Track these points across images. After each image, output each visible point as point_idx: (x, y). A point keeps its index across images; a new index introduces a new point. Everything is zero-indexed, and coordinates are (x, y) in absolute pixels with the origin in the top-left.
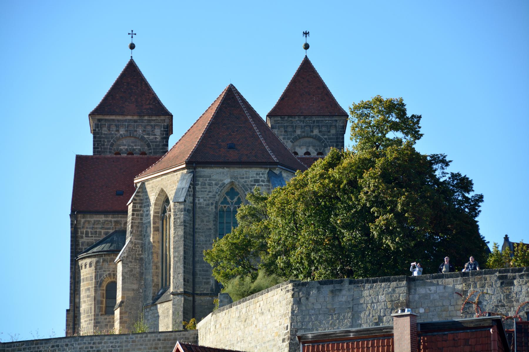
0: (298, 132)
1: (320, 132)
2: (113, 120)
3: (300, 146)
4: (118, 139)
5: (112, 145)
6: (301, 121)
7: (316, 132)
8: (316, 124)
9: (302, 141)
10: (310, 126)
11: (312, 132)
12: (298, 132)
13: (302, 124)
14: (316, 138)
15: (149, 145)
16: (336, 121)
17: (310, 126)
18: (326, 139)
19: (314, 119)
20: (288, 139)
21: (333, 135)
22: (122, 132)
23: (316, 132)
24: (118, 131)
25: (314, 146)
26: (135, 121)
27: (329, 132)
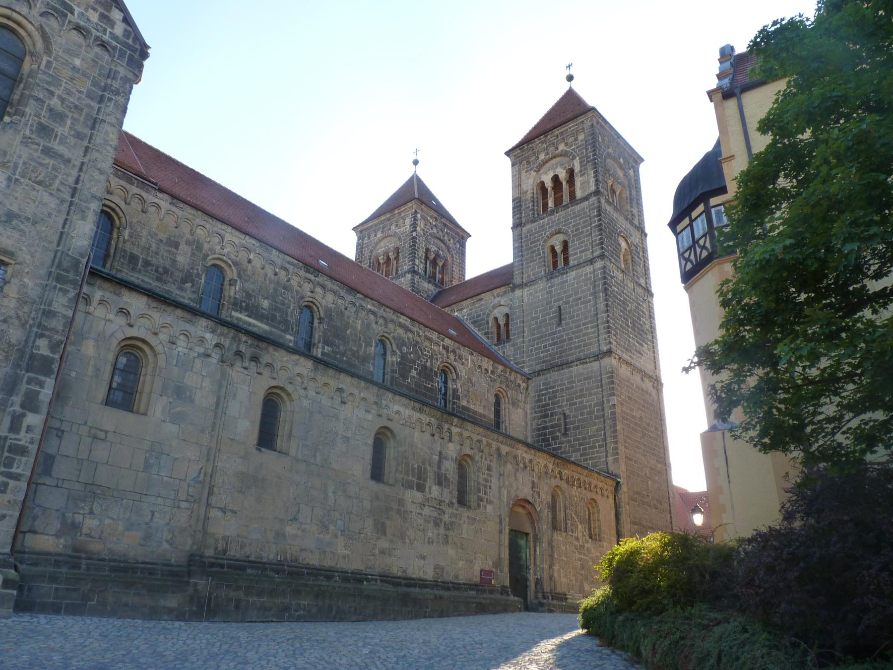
0: (542, 157)
1: (566, 144)
2: (371, 227)
3: (546, 173)
4: (377, 244)
5: (371, 252)
6: (542, 143)
7: (562, 147)
8: (560, 138)
9: (548, 165)
10: (553, 144)
11: (557, 148)
12: (542, 157)
13: (545, 145)
14: (564, 154)
15: (400, 239)
16: (583, 122)
17: (553, 144)
18: (573, 150)
19: (556, 132)
20: (531, 170)
21: (582, 141)
22: (379, 235)
23: (562, 147)
24: (376, 235)
25: (561, 165)
26: (389, 219)
27: (576, 139)
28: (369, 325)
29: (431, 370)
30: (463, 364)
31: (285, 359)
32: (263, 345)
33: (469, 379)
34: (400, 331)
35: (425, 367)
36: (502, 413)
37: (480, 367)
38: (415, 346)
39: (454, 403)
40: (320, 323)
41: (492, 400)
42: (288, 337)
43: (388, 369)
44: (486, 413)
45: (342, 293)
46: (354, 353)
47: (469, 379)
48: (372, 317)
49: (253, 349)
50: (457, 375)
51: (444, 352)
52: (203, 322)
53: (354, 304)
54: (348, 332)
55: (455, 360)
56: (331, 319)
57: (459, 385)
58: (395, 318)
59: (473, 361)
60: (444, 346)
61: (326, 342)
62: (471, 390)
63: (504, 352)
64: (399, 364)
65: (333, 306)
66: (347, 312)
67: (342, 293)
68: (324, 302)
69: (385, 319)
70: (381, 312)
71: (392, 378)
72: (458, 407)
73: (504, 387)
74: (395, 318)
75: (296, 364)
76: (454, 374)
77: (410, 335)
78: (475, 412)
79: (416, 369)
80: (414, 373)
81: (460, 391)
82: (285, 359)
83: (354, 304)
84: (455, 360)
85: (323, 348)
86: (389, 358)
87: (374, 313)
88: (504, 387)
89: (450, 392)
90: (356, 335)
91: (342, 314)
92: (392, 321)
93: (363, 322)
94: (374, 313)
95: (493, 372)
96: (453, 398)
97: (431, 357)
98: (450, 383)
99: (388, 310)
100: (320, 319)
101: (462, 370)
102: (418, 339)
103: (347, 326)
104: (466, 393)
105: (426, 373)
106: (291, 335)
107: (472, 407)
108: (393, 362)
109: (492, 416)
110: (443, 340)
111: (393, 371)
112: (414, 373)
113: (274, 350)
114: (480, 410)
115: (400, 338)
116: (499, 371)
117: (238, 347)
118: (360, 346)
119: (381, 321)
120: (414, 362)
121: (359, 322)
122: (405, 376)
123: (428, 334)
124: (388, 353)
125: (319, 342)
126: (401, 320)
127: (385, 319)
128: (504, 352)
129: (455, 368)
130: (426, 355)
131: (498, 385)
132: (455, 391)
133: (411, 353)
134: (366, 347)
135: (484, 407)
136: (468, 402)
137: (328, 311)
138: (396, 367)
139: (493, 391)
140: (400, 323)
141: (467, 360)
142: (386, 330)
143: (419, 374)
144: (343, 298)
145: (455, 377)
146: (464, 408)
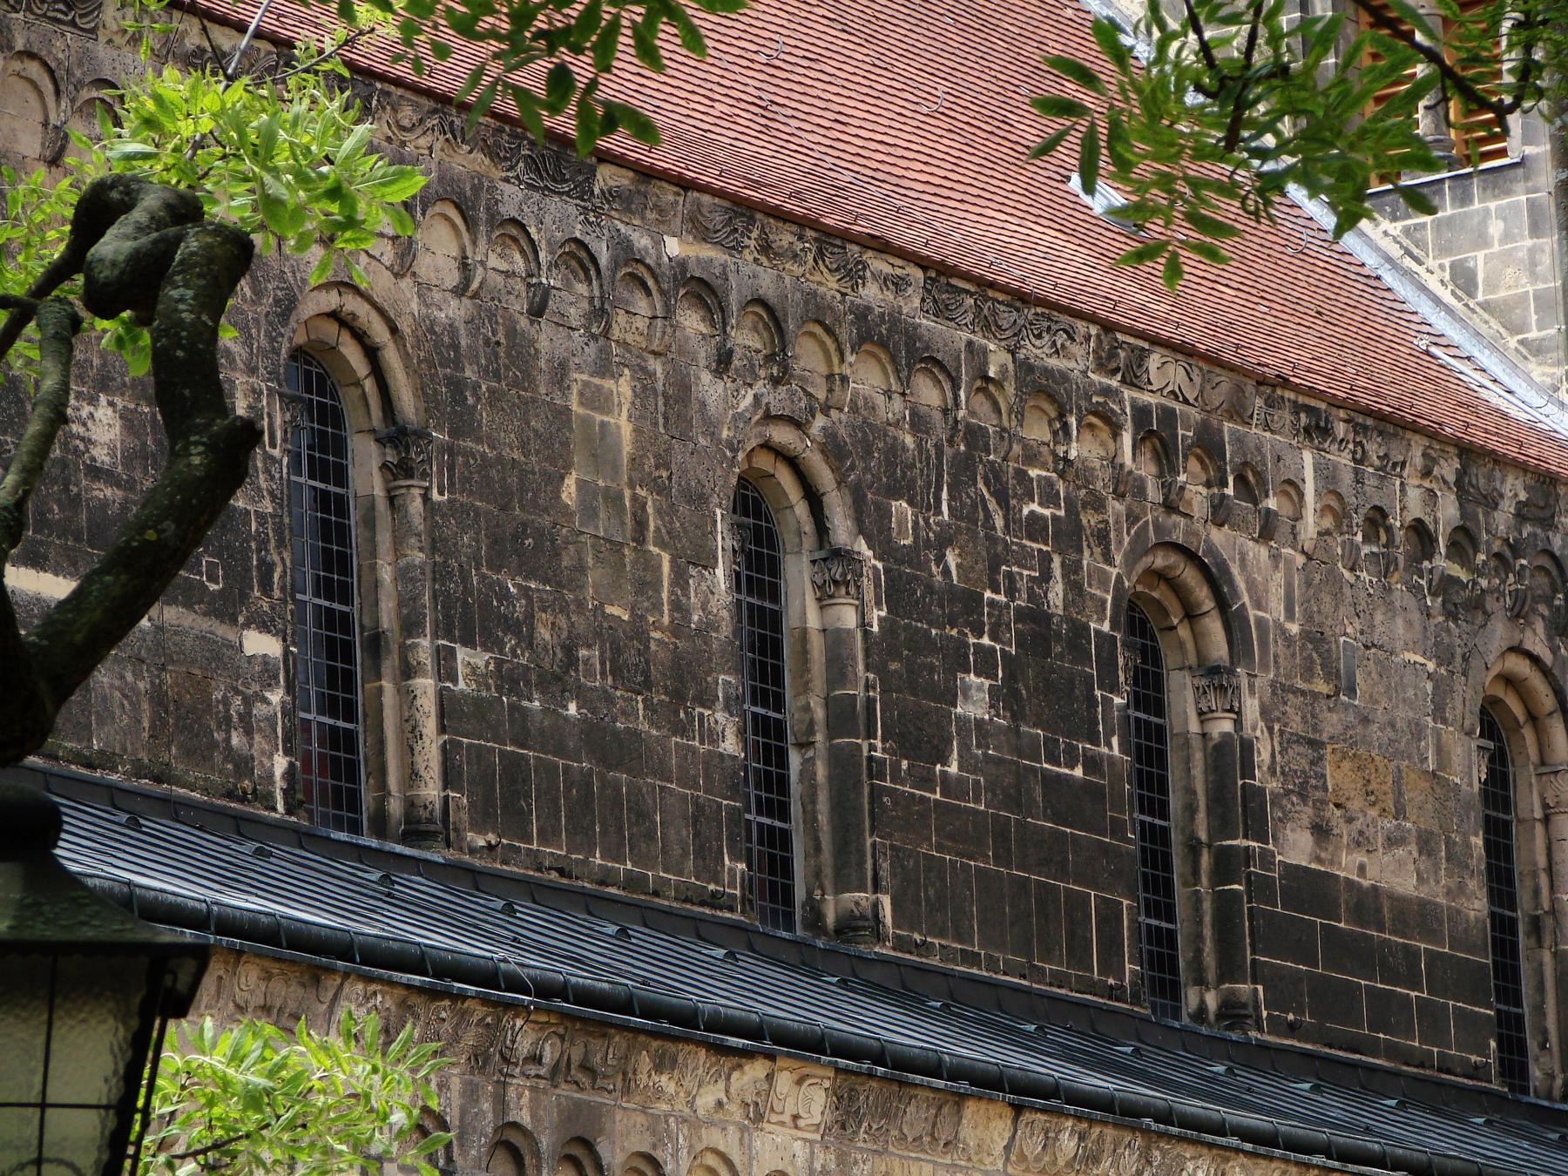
28: (682, 391)
29: (1080, 630)
30: (1266, 533)
31: (707, 1099)
32: (605, 1053)
33: (1315, 638)
34: (868, 378)
35: (1036, 616)
36: (1530, 849)
37: (1377, 520)
38: (964, 469)
39: (1227, 865)
40: (400, 471)
41: (1467, 768)
42: (261, 644)
43: (807, 703)
44: (1436, 892)
45: (512, 198)
46: (605, 632)
47: (1315, 638)
48: (692, 322)
49: (565, 1090)
50: (1234, 623)
51: (1146, 470)
52: (361, 1007)
53: (579, 258)
54: (569, 491)
55: (1220, 513)
56: (462, 425)
57: (1251, 708)
58: (829, 285)
59: (1327, 476)
60: (1141, 413)
61: (468, 620)
62: (1332, 723)
63: (1464, 280)
64: (880, 649)
65: (454, 311)
66: (547, 340)
67: (512, 198)
68: (407, 301)
69: (770, 315)
70: (748, 273)
71: (843, 763)
72: (1261, 888)
73: (1537, 641)
74: (829, 285)
75: (757, 1115)
76: (1214, 627)
77: (928, 394)
78: (1367, 903)
79: (985, 663)
80: (975, 701)
81: (1263, 754)
82: (707, 1099)
83: (579, 258)
84: (1220, 513)
85: (445, 666)
86: (803, 608)
87: (704, 291)
88: (1537, 641)
89: (1189, 776)
90: (615, 499)
91: (513, 357)
92: (819, 315)
93: (644, 391)
94: (704, 291)
95: (1464, 541)
96: (1222, 825)
97: (1068, 535)
98: (1182, 694)
99: (784, 238)
100: (396, 436)
101: (1266, 580)
102: (972, 408)
103: (556, 440)
104: (1299, 758)
105: (1044, 667)
106: (265, 626)
107: (1346, 865)
108: (835, 639)
109: (1477, 906)
110: (1133, 379)
111: (842, 717)
112: (975, 701)
113: (659, 1068)
114: (1396, 873)
115: (869, 434)
116: (1503, 518)
117: (501, 1103)
118: (647, 585)
119: (746, 338)
120: (966, 606)
121: (623, 388)
122: (922, 739)
123: (1036, 350)
124: (798, 574)
125: (410, 626)
126: (871, 293)
127: (770, 315)
128: (1464, 280)
129: (1216, 578)
130: (1035, 527)
131: (1499, 633)
132: (1230, 758)
133: (944, 540)
134: (680, 579)
135: (1426, 844)
136: (1321, 831)
137: (438, 350)
138: (861, 682)
139: (1465, 703)
140: (862, 314)
141: (1293, 487)
142: (777, 399)
143: (1004, 697)
144: (514, 231)
145: (1219, 648)
146: (1311, 888)
